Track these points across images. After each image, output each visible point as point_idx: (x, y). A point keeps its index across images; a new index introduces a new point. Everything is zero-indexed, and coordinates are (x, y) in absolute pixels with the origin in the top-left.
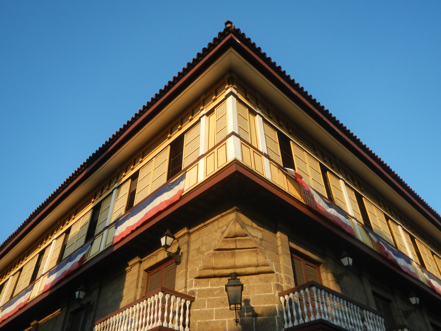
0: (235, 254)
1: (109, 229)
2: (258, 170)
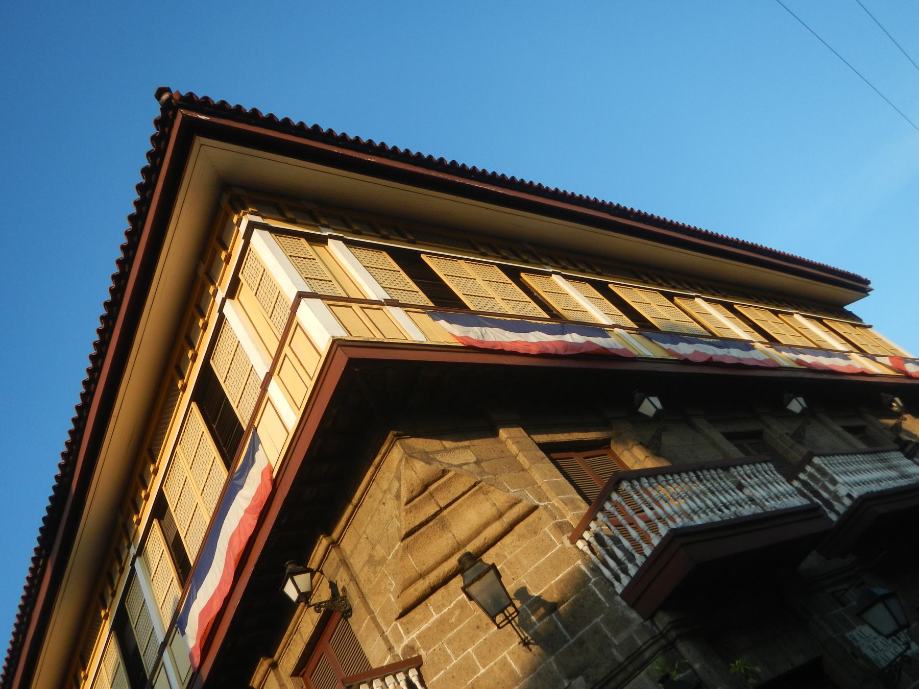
0: (446, 521)
1: (171, 645)
2: (392, 336)
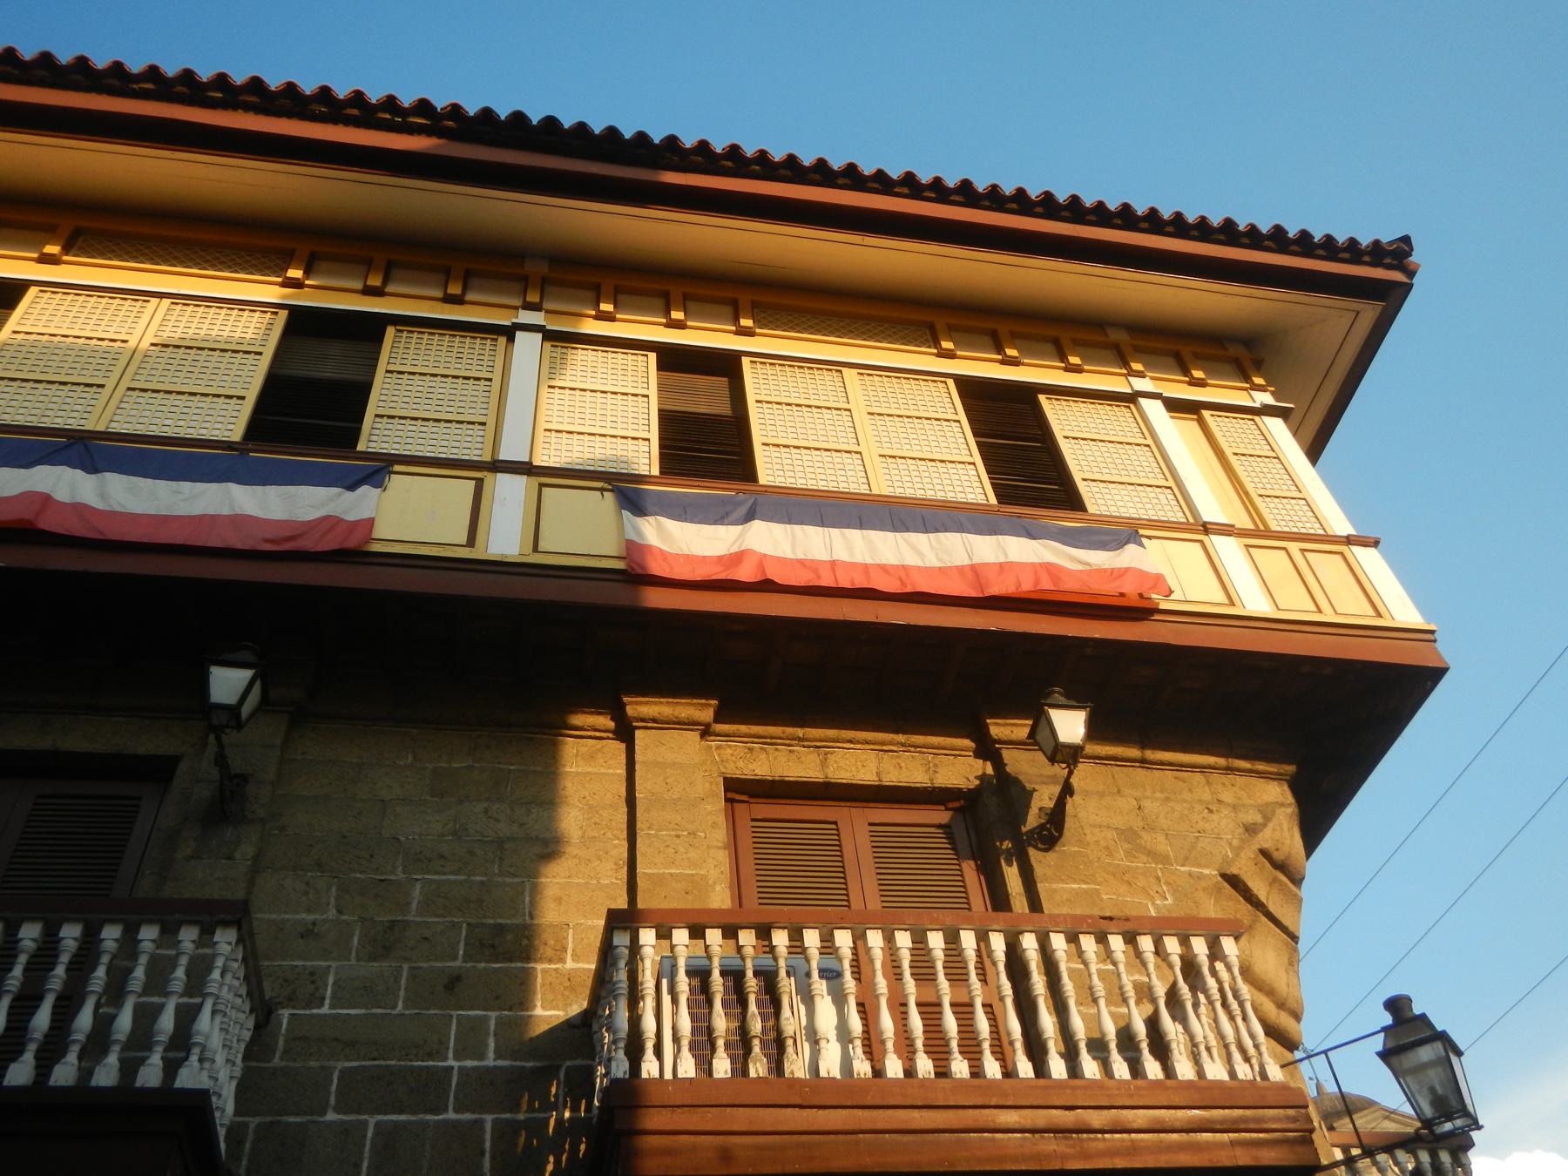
1: (541, 485)
